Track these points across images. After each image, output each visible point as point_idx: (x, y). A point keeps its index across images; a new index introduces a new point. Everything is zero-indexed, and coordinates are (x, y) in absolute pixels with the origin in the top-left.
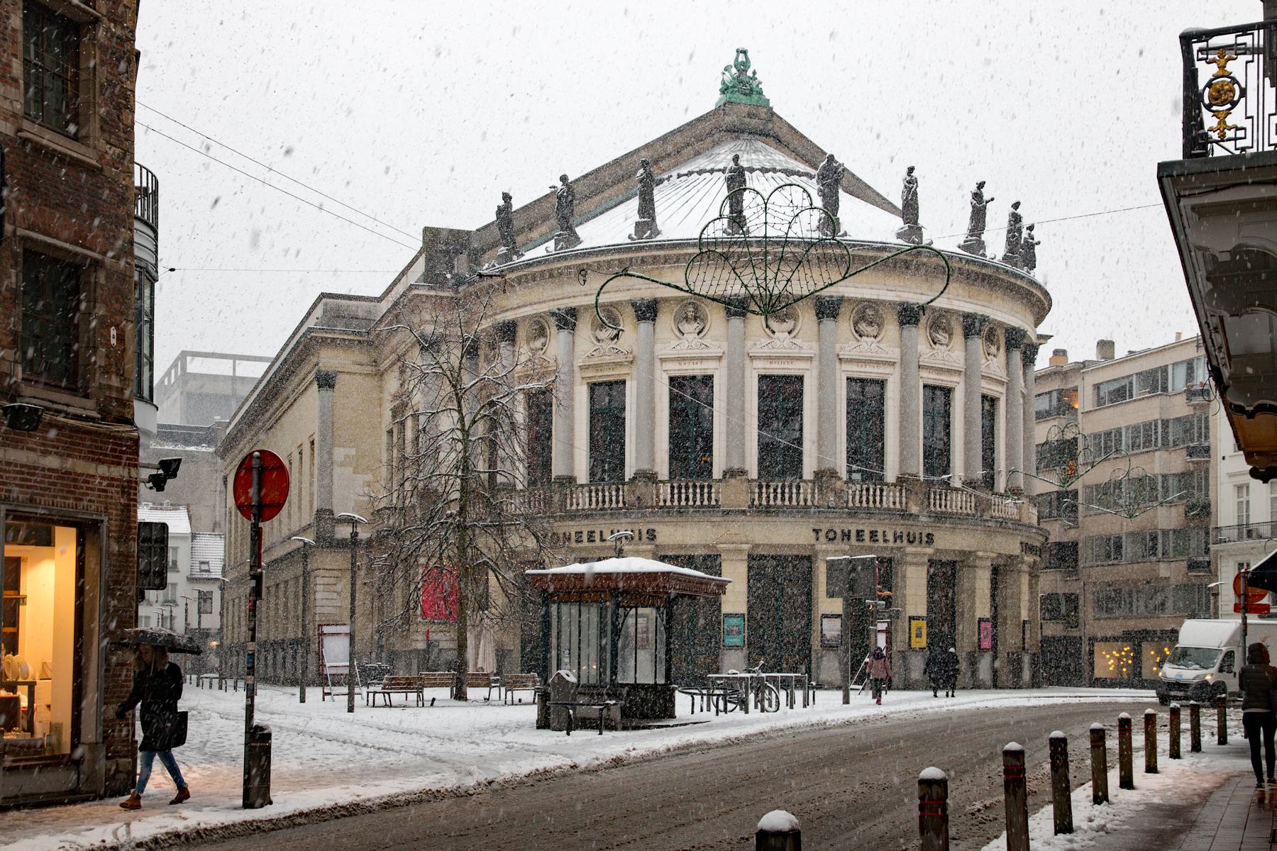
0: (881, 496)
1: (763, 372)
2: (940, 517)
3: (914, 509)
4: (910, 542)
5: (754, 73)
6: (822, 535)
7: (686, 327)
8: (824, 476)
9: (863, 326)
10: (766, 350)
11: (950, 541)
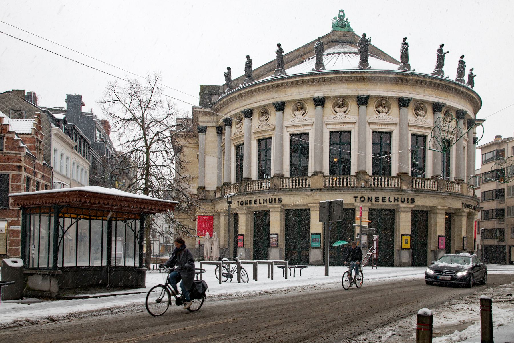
0: (388, 181)
1: (332, 130)
2: (418, 191)
3: (405, 187)
4: (402, 202)
6: (358, 199)
8: (360, 174)
9: (380, 109)
10: (333, 120)
11: (423, 202)
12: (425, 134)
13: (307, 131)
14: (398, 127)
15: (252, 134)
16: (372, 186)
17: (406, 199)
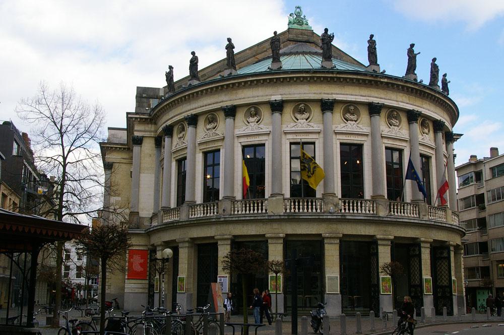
7: (251, 119)
9: (348, 115)
12: (401, 147)
13: (263, 142)
14: (370, 137)
15: (197, 145)
16: (343, 211)
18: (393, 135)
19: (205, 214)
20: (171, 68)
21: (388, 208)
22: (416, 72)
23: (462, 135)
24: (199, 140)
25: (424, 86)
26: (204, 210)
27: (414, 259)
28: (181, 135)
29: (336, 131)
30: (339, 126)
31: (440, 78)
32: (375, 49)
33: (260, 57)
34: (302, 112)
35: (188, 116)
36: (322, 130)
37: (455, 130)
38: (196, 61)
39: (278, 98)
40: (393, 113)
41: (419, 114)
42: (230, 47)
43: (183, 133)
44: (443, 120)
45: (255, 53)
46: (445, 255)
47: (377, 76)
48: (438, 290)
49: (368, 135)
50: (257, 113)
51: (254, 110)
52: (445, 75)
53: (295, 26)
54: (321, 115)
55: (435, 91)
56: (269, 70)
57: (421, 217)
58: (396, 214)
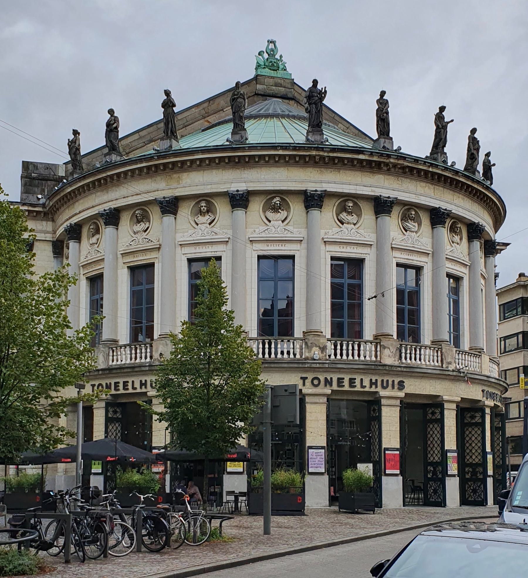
1: (261, 253)
4: (384, 388)
5: (281, 56)
6: (308, 382)
7: (201, 219)
9: (344, 216)
12: (419, 264)
16: (333, 357)
17: (390, 383)
18: (408, 245)
19: (133, 359)
20: (76, 133)
21: (398, 354)
22: (446, 150)
23: (508, 244)
24: (122, 249)
25: (457, 172)
26: (131, 354)
27: (433, 426)
28: (94, 240)
29: (325, 240)
30: (330, 231)
31: (481, 158)
32: (387, 113)
33: (213, 119)
34: (275, 209)
35: (105, 210)
36: (306, 237)
37: (499, 237)
38: (115, 125)
39: (242, 187)
40: (410, 211)
41: (448, 214)
42: (168, 104)
43: (97, 236)
44: (482, 222)
45: (206, 112)
46: (478, 419)
47: (389, 156)
48: (467, 469)
49: (371, 245)
50: (210, 210)
51: (204, 203)
52: (488, 155)
53: (267, 72)
54: (304, 214)
55: (473, 180)
56: (228, 143)
57: (444, 366)
58: (409, 361)
